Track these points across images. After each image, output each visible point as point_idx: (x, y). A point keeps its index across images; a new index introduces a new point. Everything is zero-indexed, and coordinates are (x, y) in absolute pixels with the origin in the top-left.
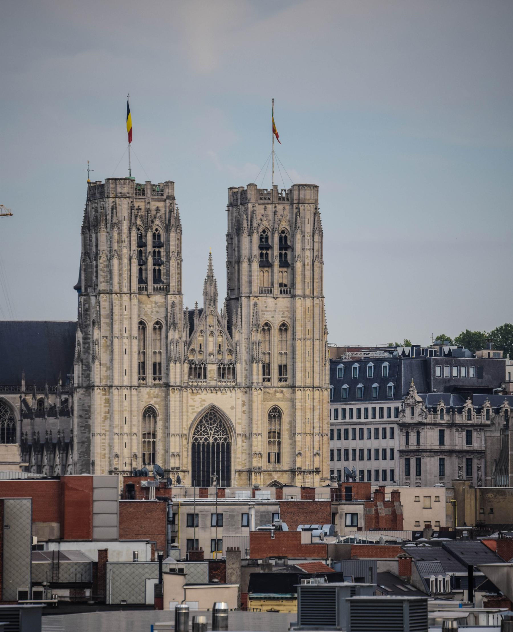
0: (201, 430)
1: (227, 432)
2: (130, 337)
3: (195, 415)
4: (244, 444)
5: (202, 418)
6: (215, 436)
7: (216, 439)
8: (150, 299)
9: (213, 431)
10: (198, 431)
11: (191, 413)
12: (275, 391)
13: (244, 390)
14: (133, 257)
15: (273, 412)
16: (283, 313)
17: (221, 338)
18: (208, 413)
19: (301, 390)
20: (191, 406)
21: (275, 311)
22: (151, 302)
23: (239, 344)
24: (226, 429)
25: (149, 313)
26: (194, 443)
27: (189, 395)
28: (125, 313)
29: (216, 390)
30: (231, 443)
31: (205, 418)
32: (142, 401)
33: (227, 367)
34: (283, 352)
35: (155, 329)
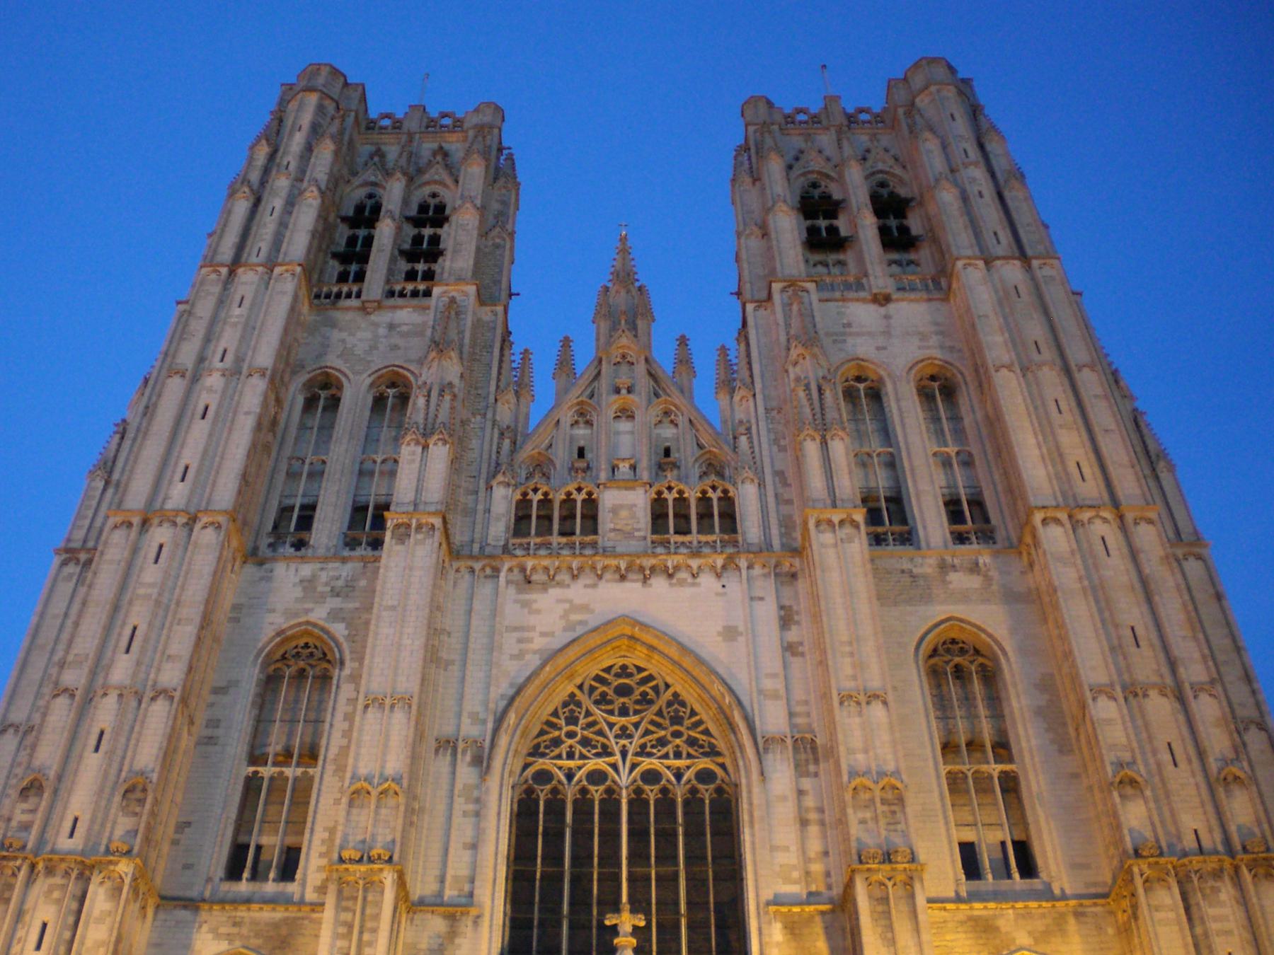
0: (571, 735)
1: (712, 746)
2: (234, 373)
3: (535, 661)
4: (807, 783)
5: (580, 687)
6: (647, 763)
7: (651, 776)
8: (373, 317)
9: (637, 741)
10: (557, 742)
11: (513, 657)
12: (944, 567)
13: (786, 567)
14: (308, 194)
15: (948, 651)
16: (923, 337)
17: (674, 431)
18: (608, 670)
19: (1057, 521)
20: (516, 629)
21: (887, 333)
22: (376, 325)
23: (749, 429)
24: (706, 732)
25: (358, 351)
26: (529, 791)
27: (509, 594)
28: (237, 311)
29: (642, 569)
30: (736, 786)
31: (592, 689)
32: (273, 611)
33: (692, 495)
34: (952, 450)
35: (379, 402)
